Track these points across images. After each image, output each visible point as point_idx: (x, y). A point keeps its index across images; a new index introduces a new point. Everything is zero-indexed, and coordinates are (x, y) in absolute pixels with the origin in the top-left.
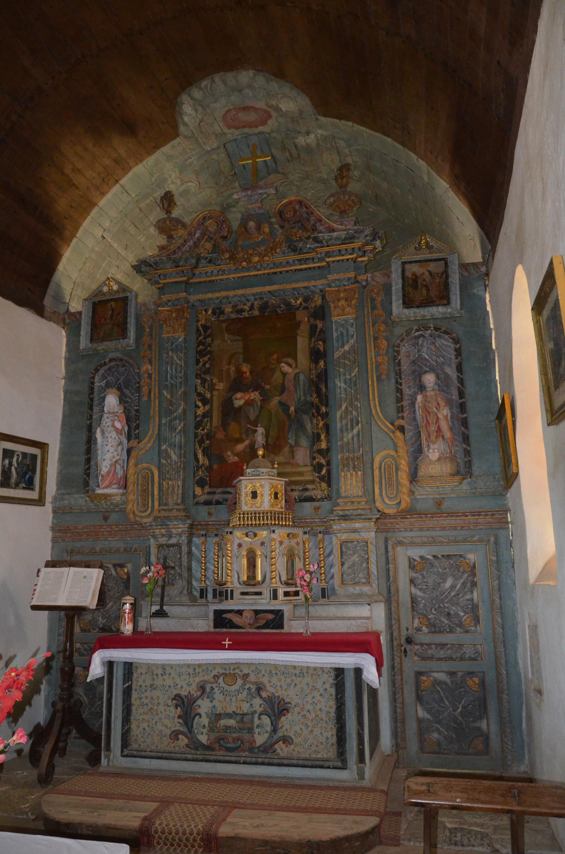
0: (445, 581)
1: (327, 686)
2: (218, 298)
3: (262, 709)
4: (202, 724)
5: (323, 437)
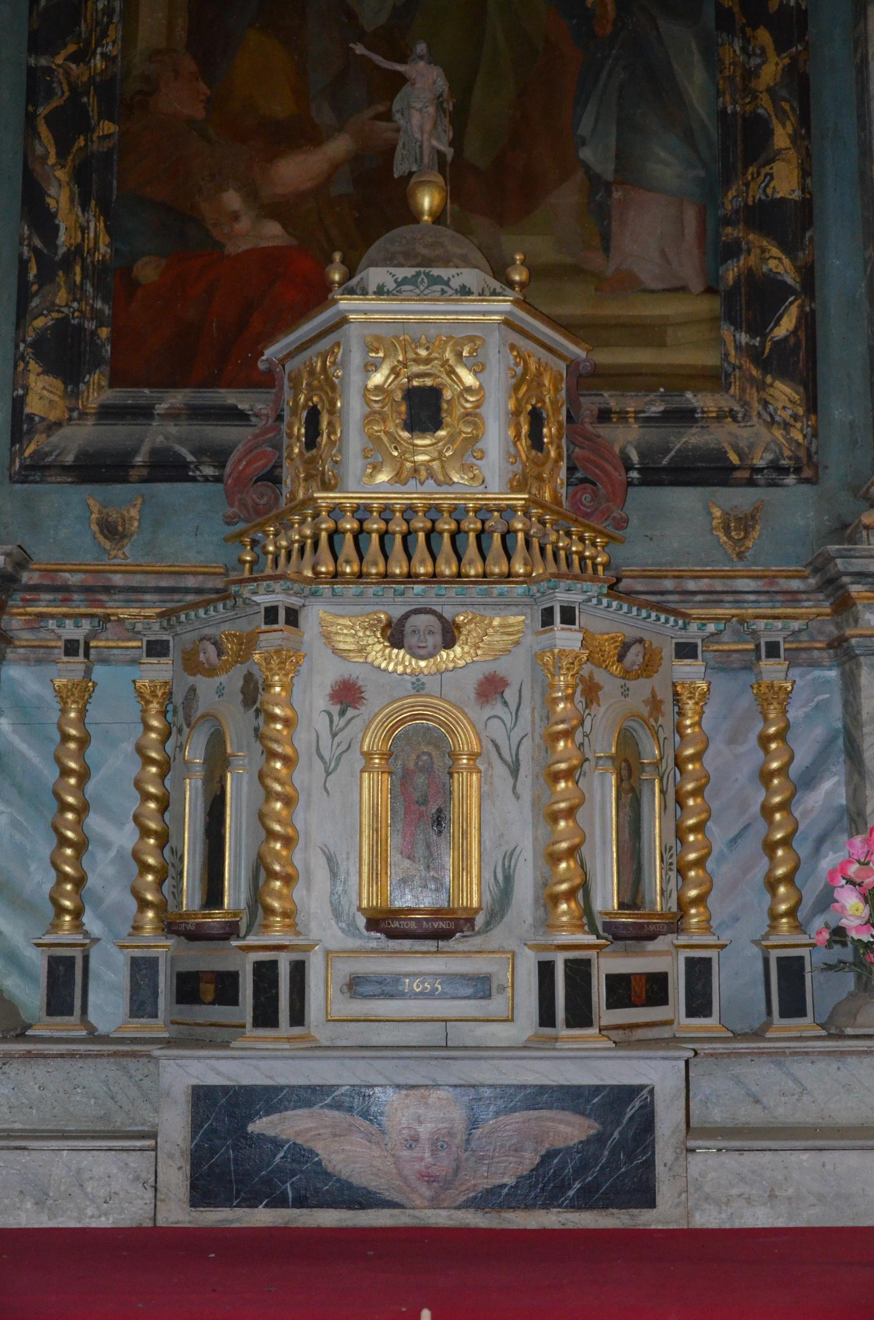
5: (781, 138)
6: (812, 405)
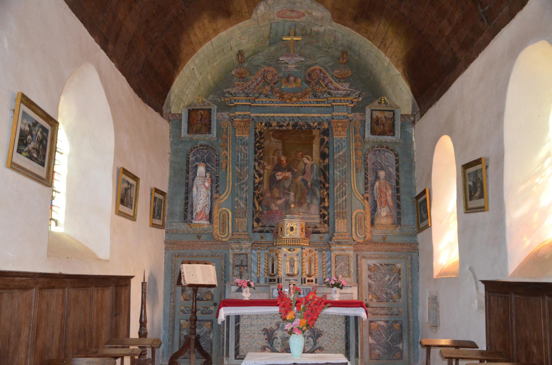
0: (385, 277)
1: (341, 323)
2: (268, 117)
3: (308, 334)
4: (278, 342)
5: (326, 200)
6: (328, 226)
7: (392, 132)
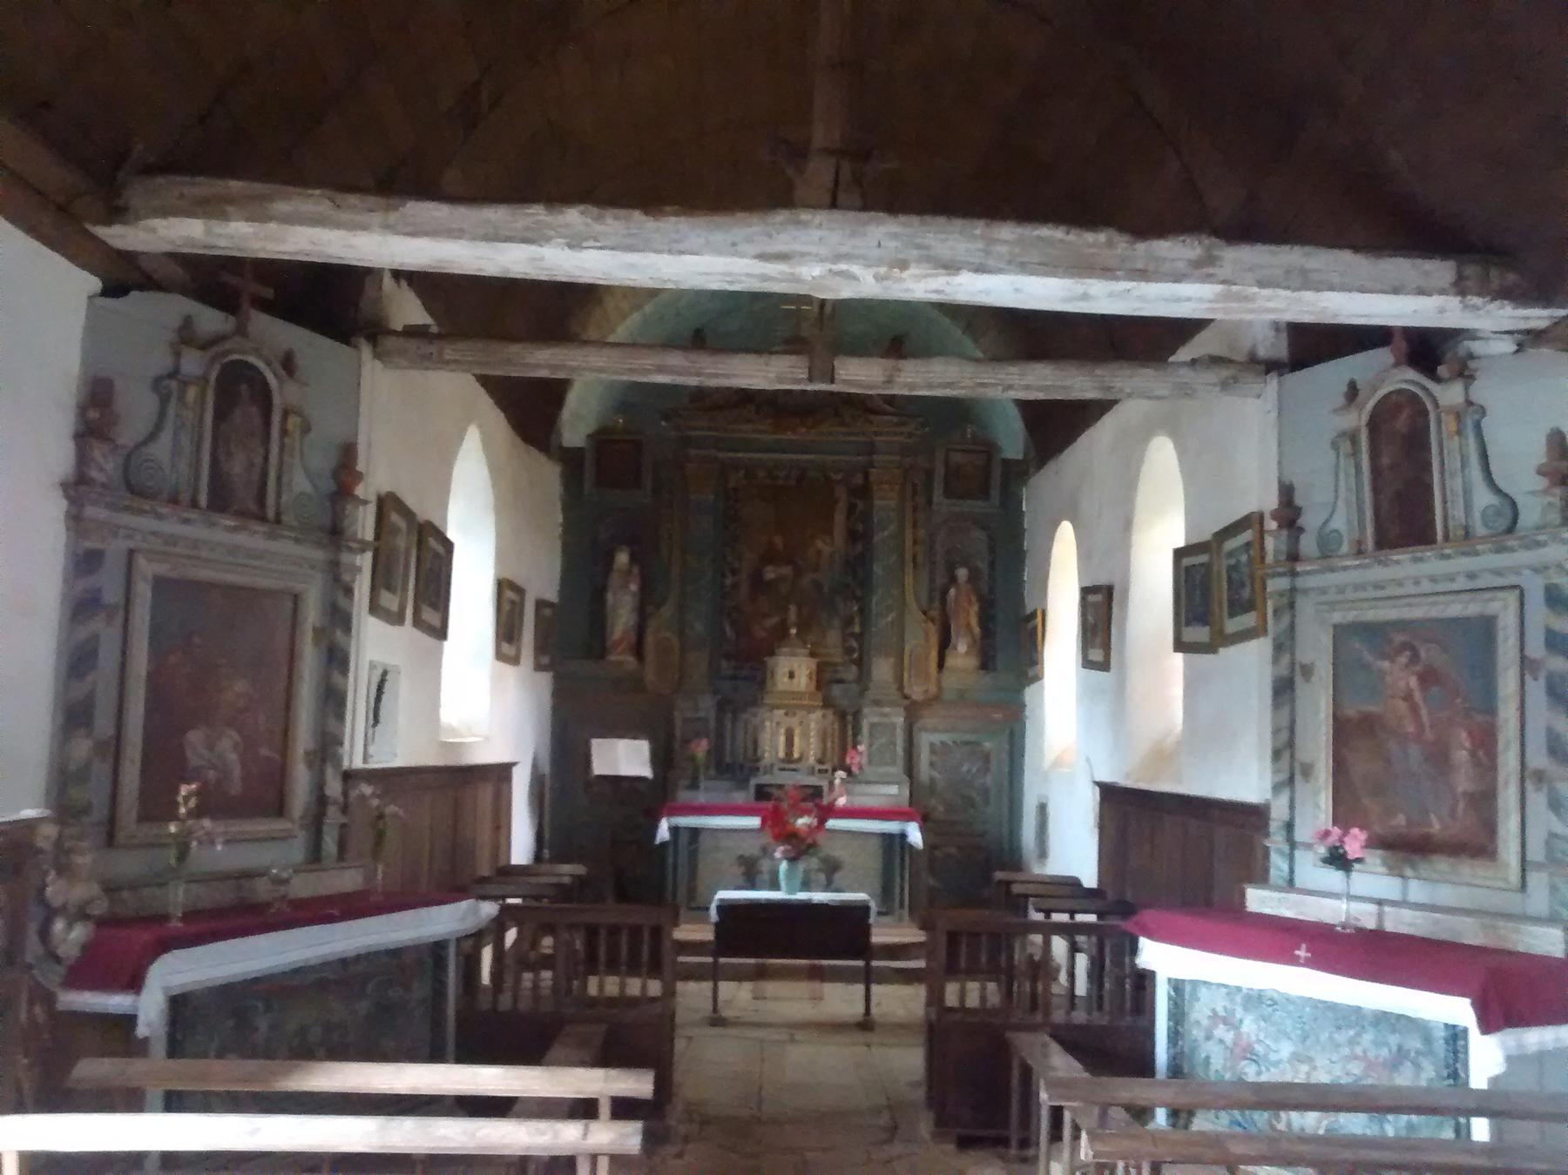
7: (985, 493)
